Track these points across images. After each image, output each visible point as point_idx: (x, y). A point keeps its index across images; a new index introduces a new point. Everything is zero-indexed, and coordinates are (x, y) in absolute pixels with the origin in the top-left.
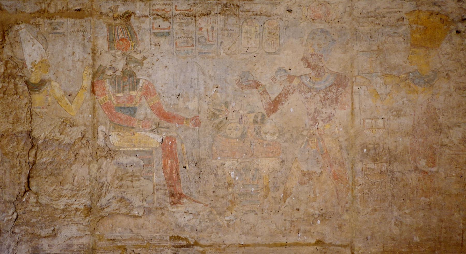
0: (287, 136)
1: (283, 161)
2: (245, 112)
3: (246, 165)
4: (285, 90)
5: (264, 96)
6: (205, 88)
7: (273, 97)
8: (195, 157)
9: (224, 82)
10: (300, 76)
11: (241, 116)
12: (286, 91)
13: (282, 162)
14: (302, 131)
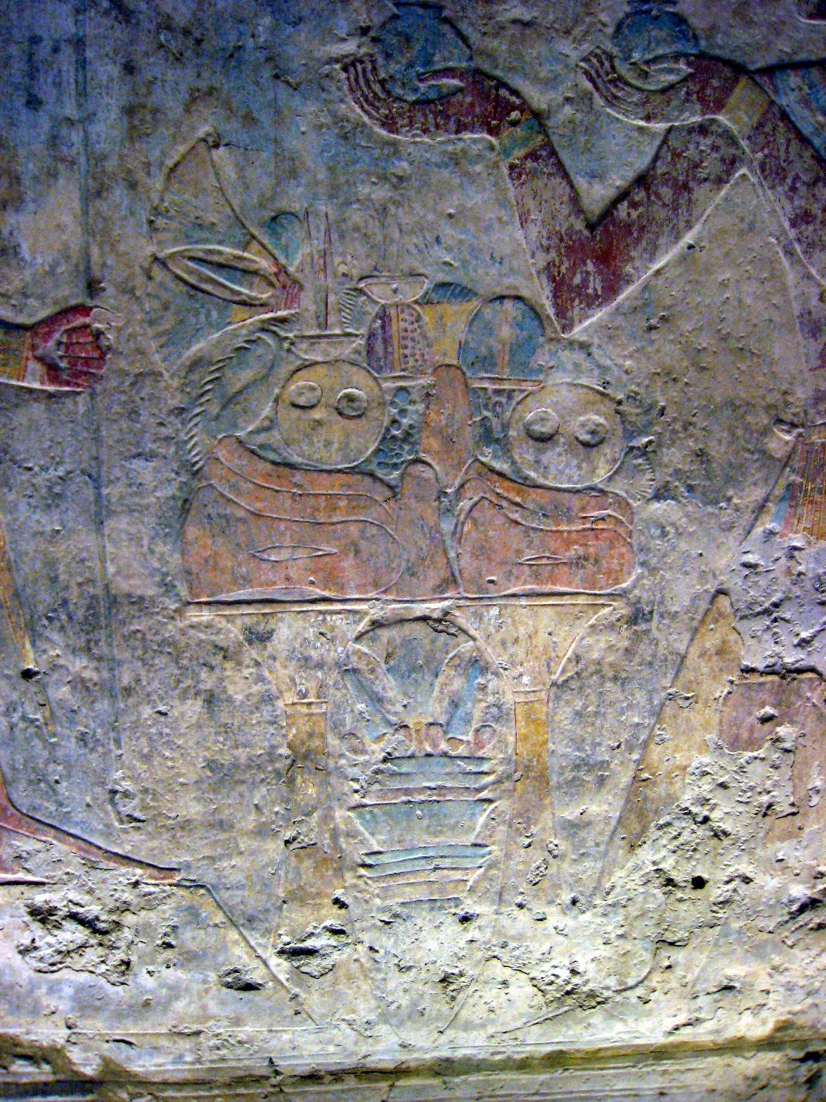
0: (674, 456)
1: (637, 616)
2: (412, 292)
3: (407, 642)
4: (676, 155)
5: (540, 183)
6: (130, 111)
7: (596, 195)
8: (75, 591)
9: (267, 73)
10: (770, 71)
11: (384, 316)
12: (682, 165)
13: (633, 620)
14: (765, 432)
